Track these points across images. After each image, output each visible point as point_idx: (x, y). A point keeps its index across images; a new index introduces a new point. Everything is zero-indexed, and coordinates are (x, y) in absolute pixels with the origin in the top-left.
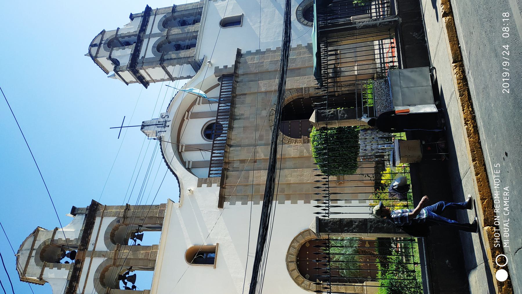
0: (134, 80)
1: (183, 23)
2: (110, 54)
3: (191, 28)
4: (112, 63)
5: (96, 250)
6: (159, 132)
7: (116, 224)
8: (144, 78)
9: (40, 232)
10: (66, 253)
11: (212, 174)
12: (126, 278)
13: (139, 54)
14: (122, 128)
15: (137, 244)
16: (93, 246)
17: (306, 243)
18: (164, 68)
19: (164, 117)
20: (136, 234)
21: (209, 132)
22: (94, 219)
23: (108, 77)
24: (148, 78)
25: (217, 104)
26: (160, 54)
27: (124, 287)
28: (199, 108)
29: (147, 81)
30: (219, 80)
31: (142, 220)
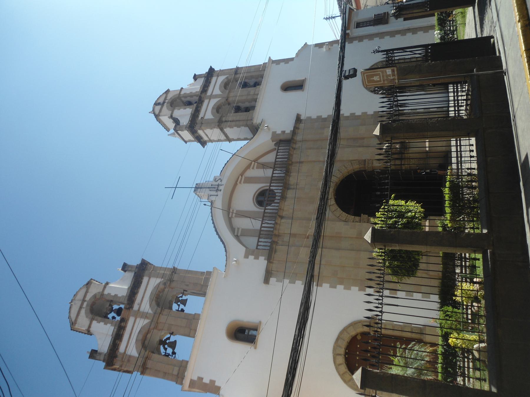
0: (193, 139)
1: (245, 85)
2: (172, 113)
3: (252, 90)
4: (173, 121)
5: (142, 309)
6: (211, 195)
7: (162, 286)
8: (202, 138)
9: (92, 284)
10: (114, 309)
11: (260, 245)
12: (166, 344)
13: (199, 114)
15: (180, 310)
16: (138, 306)
17: (357, 335)
18: (222, 130)
20: (180, 299)
21: (261, 199)
22: (142, 279)
23: (168, 135)
24: (205, 138)
25: (272, 170)
27: (163, 352)
28: (252, 173)
29: (204, 140)
30: (275, 145)
31: (187, 285)
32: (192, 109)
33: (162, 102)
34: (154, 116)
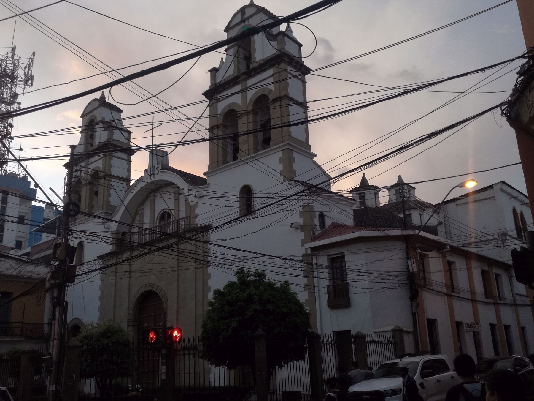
14: (154, 129)
19: (157, 170)
26: (220, 122)
32: (233, 73)
33: (246, 16)
34: (227, 24)
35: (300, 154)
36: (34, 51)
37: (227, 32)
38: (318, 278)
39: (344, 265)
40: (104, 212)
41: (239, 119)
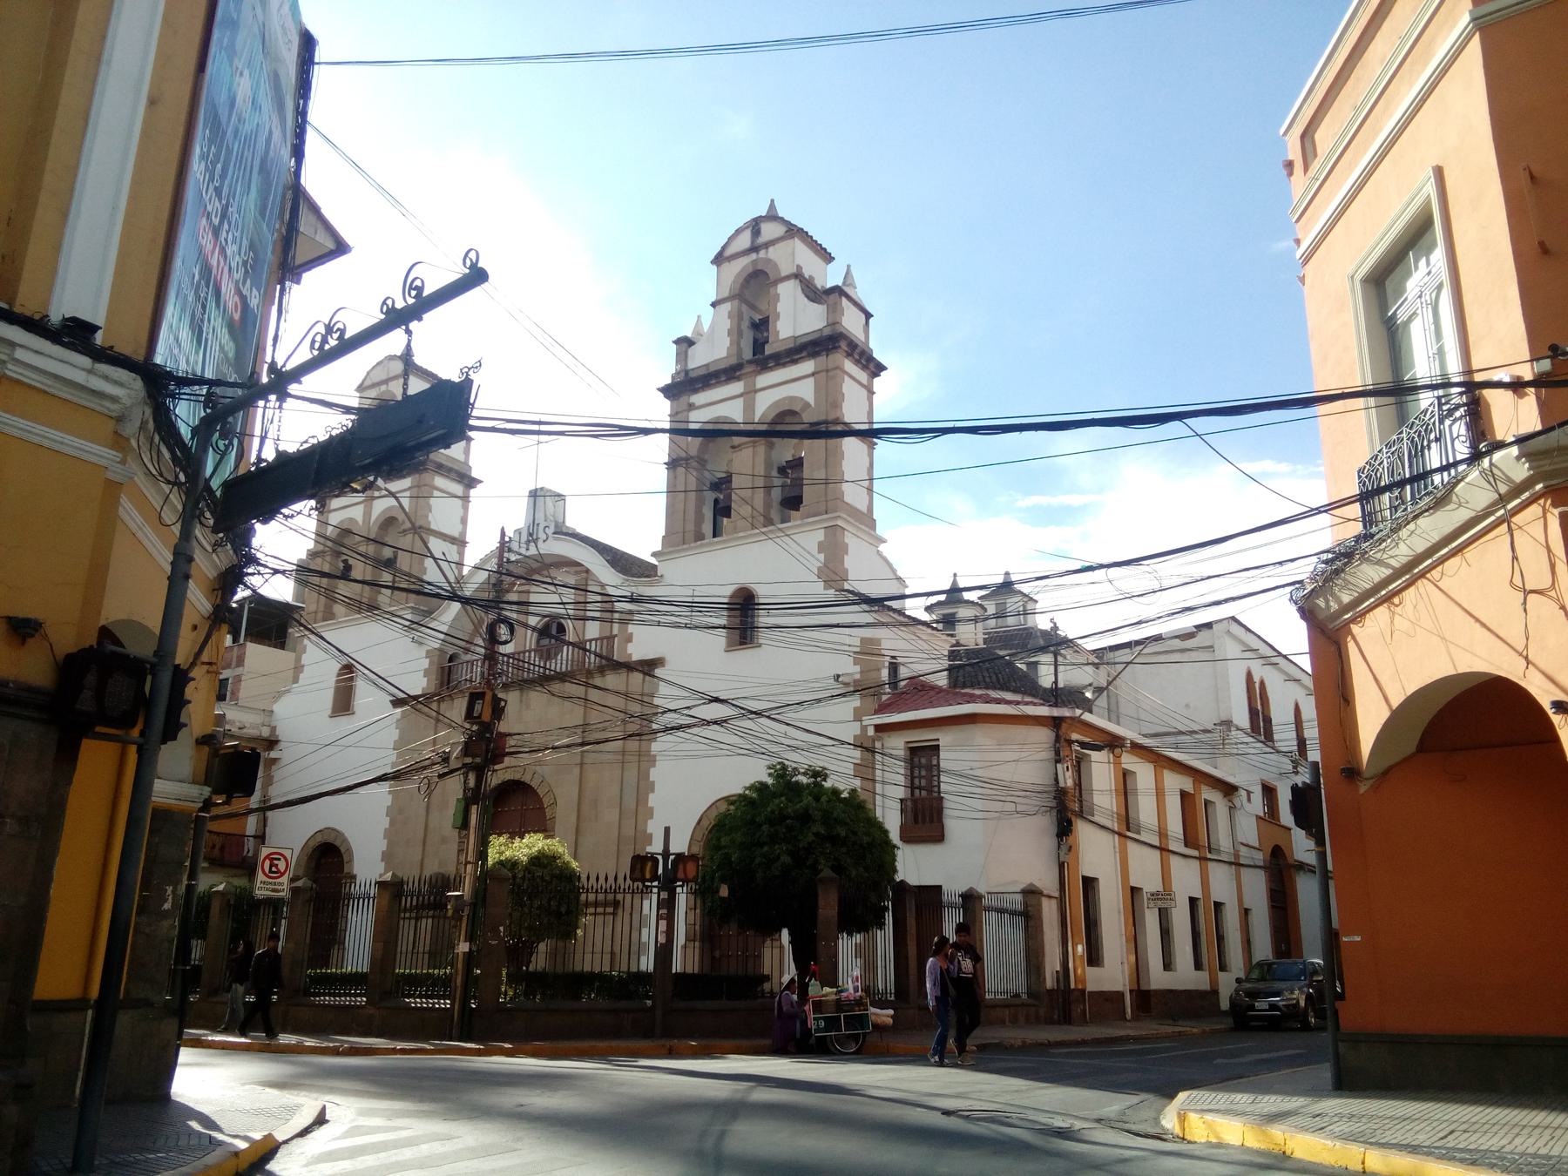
6: (520, 533)
22: (409, 474)
33: (761, 240)
35: (858, 537)
36: (422, 322)
37: (718, 266)
38: (883, 782)
39: (935, 762)
40: (412, 608)
41: (735, 452)
